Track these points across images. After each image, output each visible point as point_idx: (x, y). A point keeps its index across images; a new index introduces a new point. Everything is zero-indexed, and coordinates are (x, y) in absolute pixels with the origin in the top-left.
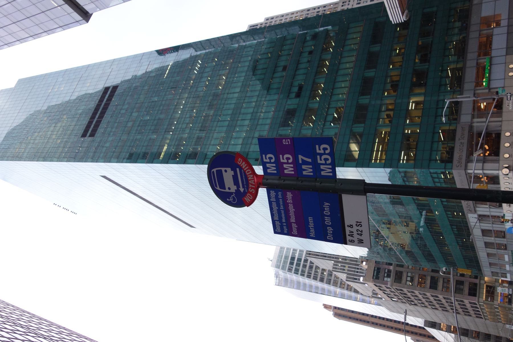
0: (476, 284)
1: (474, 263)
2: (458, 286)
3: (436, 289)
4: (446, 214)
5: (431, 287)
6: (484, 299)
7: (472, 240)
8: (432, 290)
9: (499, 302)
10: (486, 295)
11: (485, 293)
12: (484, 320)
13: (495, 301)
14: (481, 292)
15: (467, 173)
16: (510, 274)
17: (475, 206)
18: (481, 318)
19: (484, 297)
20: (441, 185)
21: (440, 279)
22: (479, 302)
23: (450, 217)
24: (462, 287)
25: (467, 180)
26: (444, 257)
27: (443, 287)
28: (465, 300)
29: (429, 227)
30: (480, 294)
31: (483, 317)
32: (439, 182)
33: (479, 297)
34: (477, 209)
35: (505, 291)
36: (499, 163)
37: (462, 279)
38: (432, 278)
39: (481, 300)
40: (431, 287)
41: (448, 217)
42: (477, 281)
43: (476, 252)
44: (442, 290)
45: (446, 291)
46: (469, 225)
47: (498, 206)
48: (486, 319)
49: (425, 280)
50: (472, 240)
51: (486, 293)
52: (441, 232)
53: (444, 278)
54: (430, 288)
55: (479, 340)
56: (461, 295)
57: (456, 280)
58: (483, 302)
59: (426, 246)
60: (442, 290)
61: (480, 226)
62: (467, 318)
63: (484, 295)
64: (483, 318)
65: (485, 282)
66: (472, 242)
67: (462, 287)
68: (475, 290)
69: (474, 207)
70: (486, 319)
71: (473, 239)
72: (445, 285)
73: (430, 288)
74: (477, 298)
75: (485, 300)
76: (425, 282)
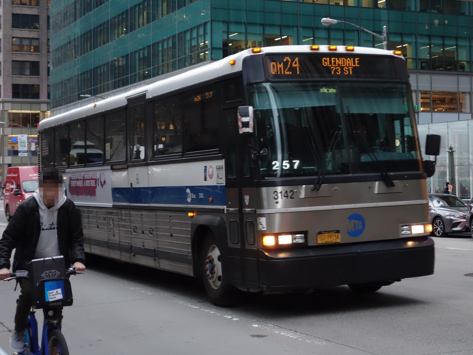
0: (37, 96)
1: (139, 70)
2: (28, 65)
3: (13, 26)
4: (168, 39)
5: (15, 16)
6: (10, 111)
7: (85, 98)
8: (10, 18)
9: (10, 136)
10: (19, 113)
11: (23, 111)
13: (10, 129)
14: (24, 105)
19: (14, 111)
20: (189, 40)
21: (37, 32)
23: (163, 45)
24: (28, 72)
26: (124, 16)
27: (21, 39)
29: (120, 18)
30: (19, 105)
32: (191, 39)
35: (22, 146)
37: (43, 71)
38: (35, 18)
40: (15, 16)
41: (163, 41)
42: (43, 97)
43: (119, 87)
44: (13, 38)
45: (13, 44)
46: (130, 86)
49: (28, 3)
50: (85, 98)
51: (23, 113)
52: (158, 18)
53: (38, 39)
54: (13, 15)
56: (11, 71)
57: (38, 62)
58: (5, 109)
59: (87, 11)
60: (13, 38)
63: (19, 111)
65: (44, 112)
66: (82, 98)
67: (28, 73)
68: (25, 96)
71: (84, 100)
72: (26, 43)
73: (13, 15)
74: (10, 99)
75: (9, 114)
76: (25, 4)
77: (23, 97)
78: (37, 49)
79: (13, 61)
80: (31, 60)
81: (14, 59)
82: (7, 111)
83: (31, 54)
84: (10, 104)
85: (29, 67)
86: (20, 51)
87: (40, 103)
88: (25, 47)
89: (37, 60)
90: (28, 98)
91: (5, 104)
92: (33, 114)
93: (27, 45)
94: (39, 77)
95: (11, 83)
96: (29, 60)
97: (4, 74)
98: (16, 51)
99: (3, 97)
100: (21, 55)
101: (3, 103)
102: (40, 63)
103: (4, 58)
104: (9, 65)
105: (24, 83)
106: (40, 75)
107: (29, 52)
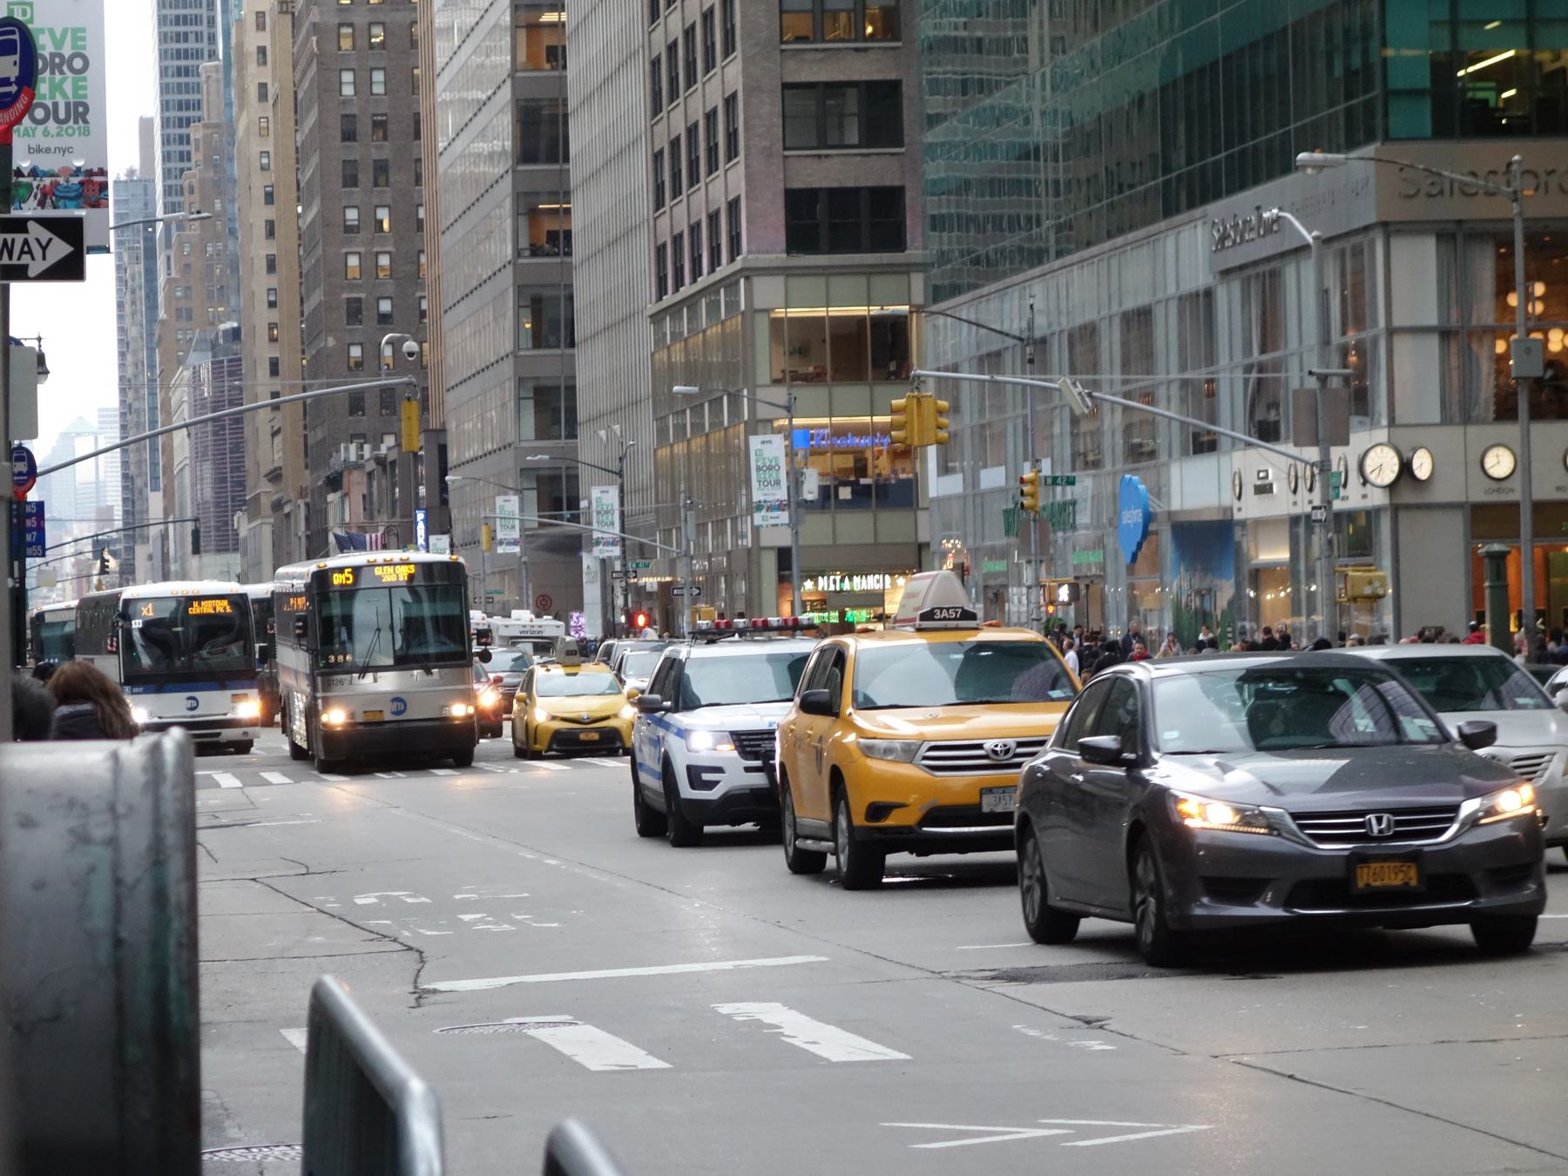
2: (852, 102)
6: (780, 313)
12: (652, 308)
15: (1372, 234)
16: (964, 497)
17: (1251, 272)
18: (662, 291)
22: (748, 273)
25: (1347, 235)
28: (741, 168)
31: (669, 299)
33: (787, 272)
34: (1236, 286)
36: (1446, 420)
39: (768, 292)
45: (782, 12)
47: (1259, 416)
48: (656, 318)
51: (837, 321)
55: (518, 253)
58: (758, 304)
61: (1167, 300)
62: (639, 171)
63: (820, 312)
64: (660, 299)
67: (855, 140)
69: (1241, 268)
70: (656, 318)
74: (779, 258)
75: (776, 323)
77: (834, 249)
78: (891, 26)
79: (786, 86)
80: (864, 78)
81: (789, 79)
82: (767, 311)
83: (866, 50)
84: (779, 281)
85: (856, 111)
86: (814, 42)
87: (906, 269)
88: (843, 17)
89: (893, 76)
90: (855, 248)
91: (759, 283)
92: (877, 321)
93: (848, 11)
94: (903, 150)
95: (780, 187)
96: (855, 78)
97: (747, 147)
98: (799, 39)
99: (749, 252)
100: (822, 55)
101: (747, 278)
102: (904, 88)
103: (746, 73)
104: (770, 108)
105: (835, 185)
106: (906, 140)
107: (855, 40)
